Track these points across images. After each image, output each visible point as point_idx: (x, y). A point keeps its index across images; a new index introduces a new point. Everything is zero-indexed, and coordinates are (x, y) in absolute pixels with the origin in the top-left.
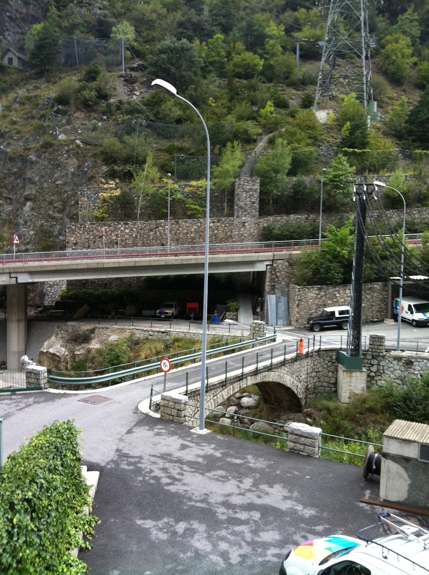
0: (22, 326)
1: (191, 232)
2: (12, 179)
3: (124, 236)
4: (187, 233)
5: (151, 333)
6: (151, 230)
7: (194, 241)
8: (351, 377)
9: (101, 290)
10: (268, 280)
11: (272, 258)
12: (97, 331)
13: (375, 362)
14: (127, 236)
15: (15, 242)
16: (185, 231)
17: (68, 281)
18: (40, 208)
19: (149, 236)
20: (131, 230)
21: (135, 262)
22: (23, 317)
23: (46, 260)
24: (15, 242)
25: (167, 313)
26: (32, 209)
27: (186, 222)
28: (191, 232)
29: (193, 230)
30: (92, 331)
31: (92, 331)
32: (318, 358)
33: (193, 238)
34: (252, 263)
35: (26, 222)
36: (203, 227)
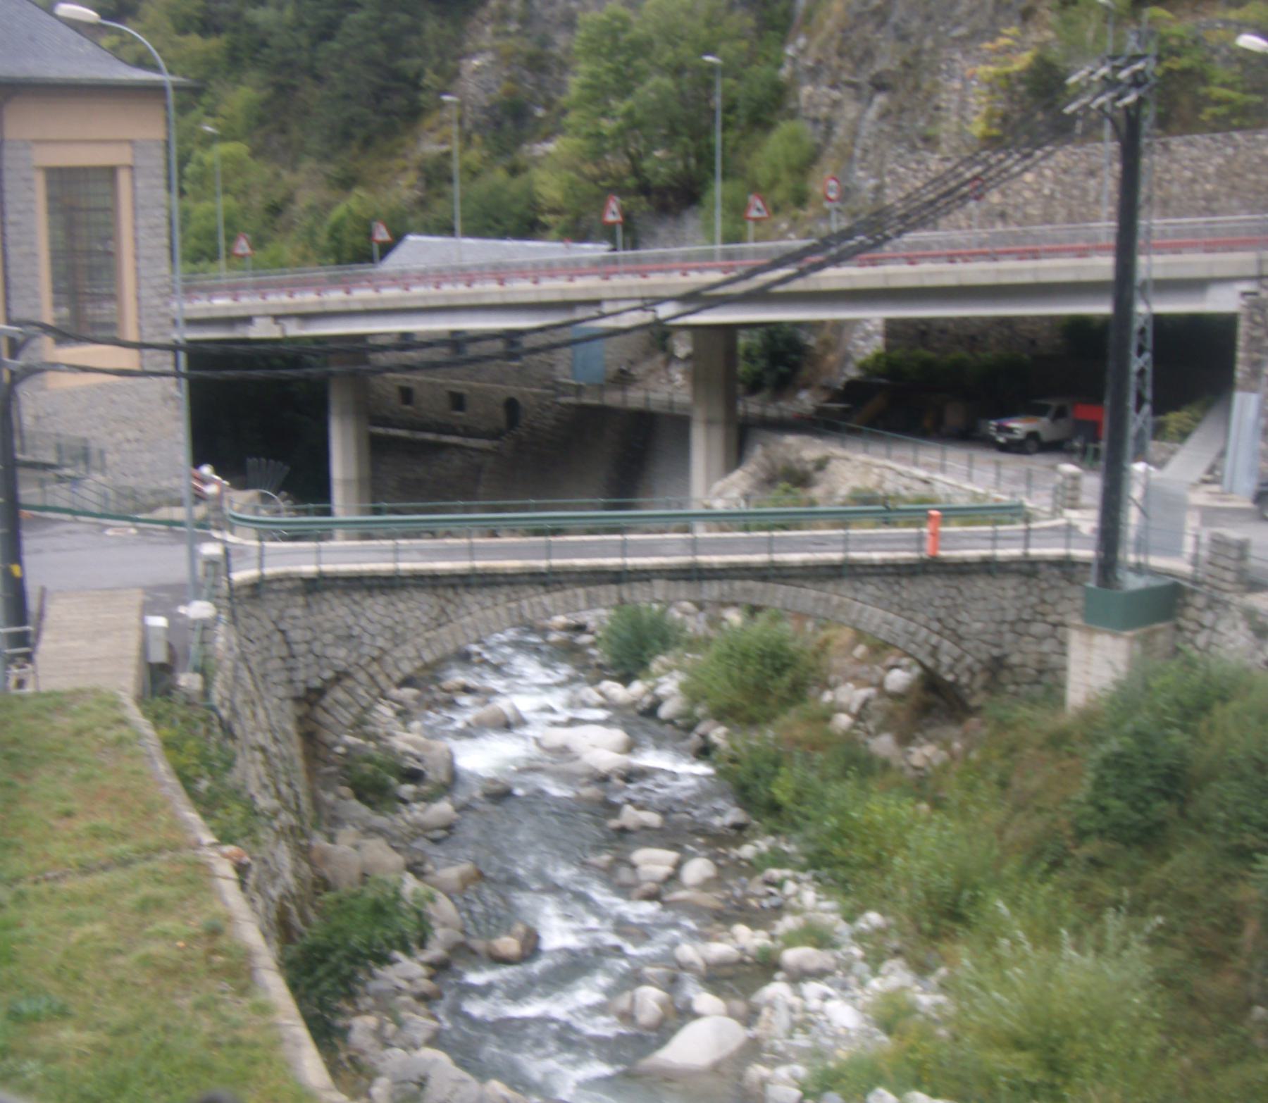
0: (718, 435)
1: (1206, 178)
2: (870, 27)
3: (1019, 193)
4: (1194, 181)
5: (906, 481)
6: (1092, 173)
7: (1215, 206)
8: (1090, 646)
9: (961, 353)
10: (1241, 342)
11: (1252, 271)
12: (833, 466)
13: (1208, 618)
14: (1028, 194)
15: (754, 214)
16: (1188, 174)
17: (889, 322)
18: (902, 110)
19: (1085, 191)
20: (1041, 175)
21: (887, 276)
22: (719, 412)
23: (660, 271)
24: (754, 214)
25: (1010, 430)
26: (884, 115)
27: (1190, 144)
28: (1206, 178)
29: (1211, 170)
30: (821, 465)
31: (821, 465)
32: (1063, 584)
33: (1209, 198)
34: (1197, 285)
35: (866, 151)
36: (1241, 158)
